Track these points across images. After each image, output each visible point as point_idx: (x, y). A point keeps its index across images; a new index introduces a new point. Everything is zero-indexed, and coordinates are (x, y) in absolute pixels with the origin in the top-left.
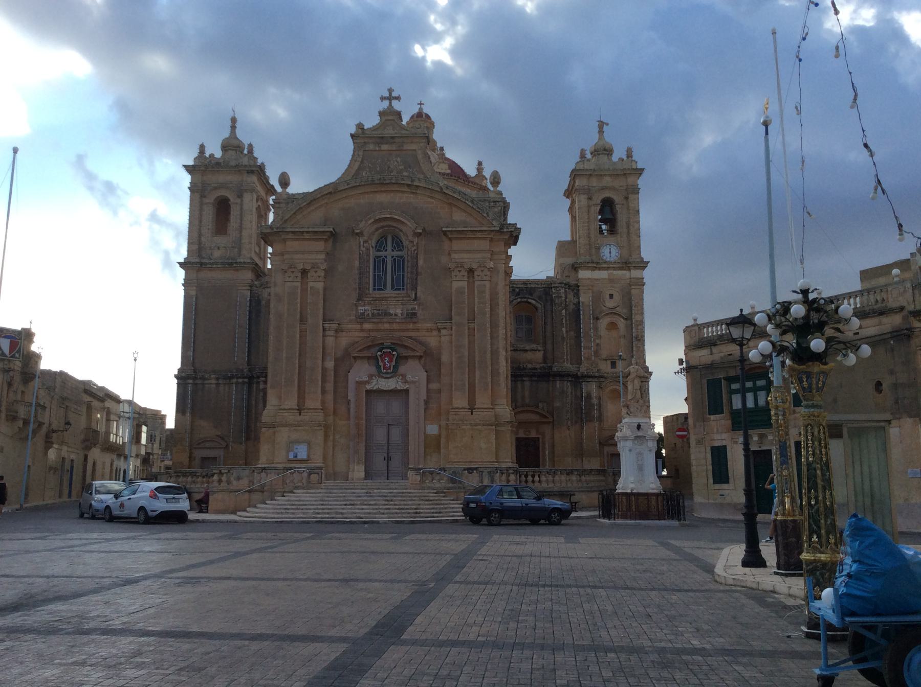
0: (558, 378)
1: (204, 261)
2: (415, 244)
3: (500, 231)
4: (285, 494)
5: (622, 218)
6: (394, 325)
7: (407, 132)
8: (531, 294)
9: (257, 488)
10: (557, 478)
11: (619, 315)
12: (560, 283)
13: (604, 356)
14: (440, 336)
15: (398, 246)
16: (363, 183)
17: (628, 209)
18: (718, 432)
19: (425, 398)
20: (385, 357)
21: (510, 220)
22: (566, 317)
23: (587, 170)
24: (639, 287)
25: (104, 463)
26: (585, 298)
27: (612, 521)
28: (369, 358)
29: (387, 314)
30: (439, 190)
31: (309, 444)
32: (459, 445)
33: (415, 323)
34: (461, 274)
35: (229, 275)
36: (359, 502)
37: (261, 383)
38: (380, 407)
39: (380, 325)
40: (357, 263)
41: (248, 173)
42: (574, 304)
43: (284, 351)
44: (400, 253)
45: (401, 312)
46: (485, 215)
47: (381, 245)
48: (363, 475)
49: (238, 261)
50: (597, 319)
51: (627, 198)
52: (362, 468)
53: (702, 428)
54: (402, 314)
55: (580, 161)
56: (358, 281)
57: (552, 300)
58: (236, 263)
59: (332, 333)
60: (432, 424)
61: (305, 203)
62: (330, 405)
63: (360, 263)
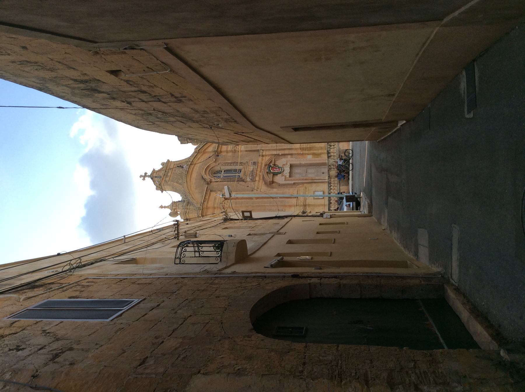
6: (258, 169)
16: (186, 178)
29: (253, 171)
31: (315, 191)
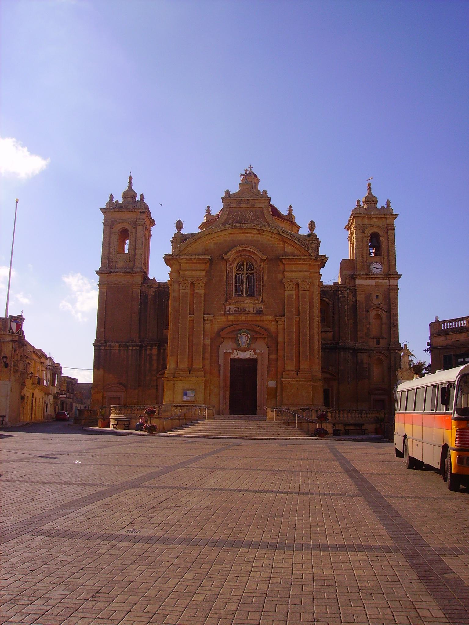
1: (112, 270)
5: (384, 246)
10: (353, 415)
12: (344, 288)
19: (268, 364)
22: (348, 310)
24: (395, 291)
26: (360, 298)
28: (232, 338)
30: (278, 233)
32: (290, 394)
34: (291, 286)
37: (148, 350)
40: (225, 278)
41: (140, 213)
42: (353, 301)
45: (253, 309)
50: (368, 311)
51: (387, 233)
54: (253, 311)
57: (339, 299)
59: (208, 322)
61: (194, 241)
62: (208, 367)
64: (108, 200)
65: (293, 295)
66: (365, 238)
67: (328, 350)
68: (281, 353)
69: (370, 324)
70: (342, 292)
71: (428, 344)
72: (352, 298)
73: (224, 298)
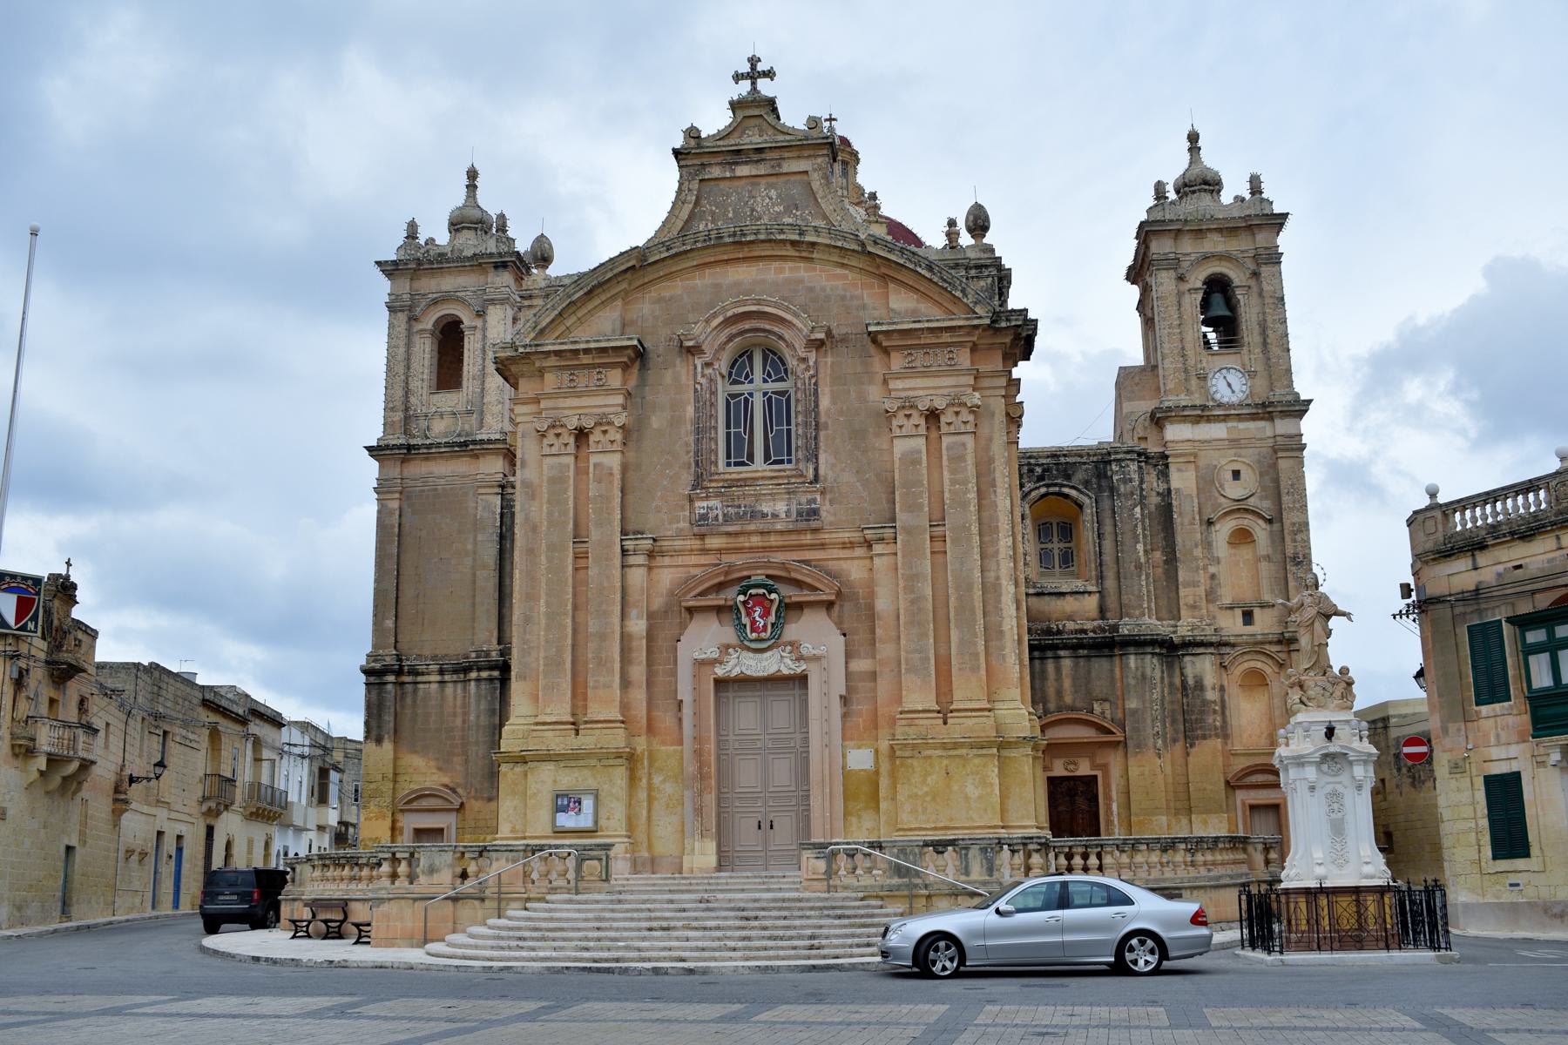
0: (1132, 650)
1: (413, 442)
2: (811, 363)
3: (993, 328)
4: (528, 905)
6: (772, 538)
7: (788, 138)
8: (1068, 477)
9: (471, 891)
11: (1254, 513)
12: (1128, 452)
13: (1227, 601)
14: (871, 558)
15: (777, 372)
16: (699, 245)
17: (1261, 294)
18: (1498, 744)
19: (844, 693)
20: (754, 606)
21: (1013, 303)
22: (1143, 521)
23: (1172, 221)
25: (250, 843)
26: (1182, 480)
27: (1275, 957)
28: (719, 610)
29: (755, 515)
31: (597, 797)
32: (920, 793)
33: (815, 531)
35: (460, 467)
36: (681, 924)
38: (746, 713)
39: (741, 539)
40: (690, 410)
42: (1158, 494)
43: (542, 601)
44: (780, 386)
45: (785, 508)
46: (959, 294)
47: (739, 367)
48: (712, 860)
49: (479, 437)
50: (1210, 523)
52: (711, 846)
53: (1463, 733)
54: (788, 513)
55: (1156, 206)
56: (692, 448)
57: (1112, 489)
58: (474, 442)
59: (641, 559)
60: (859, 748)
61: (581, 293)
63: (697, 409)
64: (400, 237)
65: (919, 452)
66: (1187, 296)
67: (1086, 651)
68: (885, 650)
69: (1218, 563)
70: (1121, 467)
71: (1406, 590)
72: (1155, 484)
73: (687, 478)
